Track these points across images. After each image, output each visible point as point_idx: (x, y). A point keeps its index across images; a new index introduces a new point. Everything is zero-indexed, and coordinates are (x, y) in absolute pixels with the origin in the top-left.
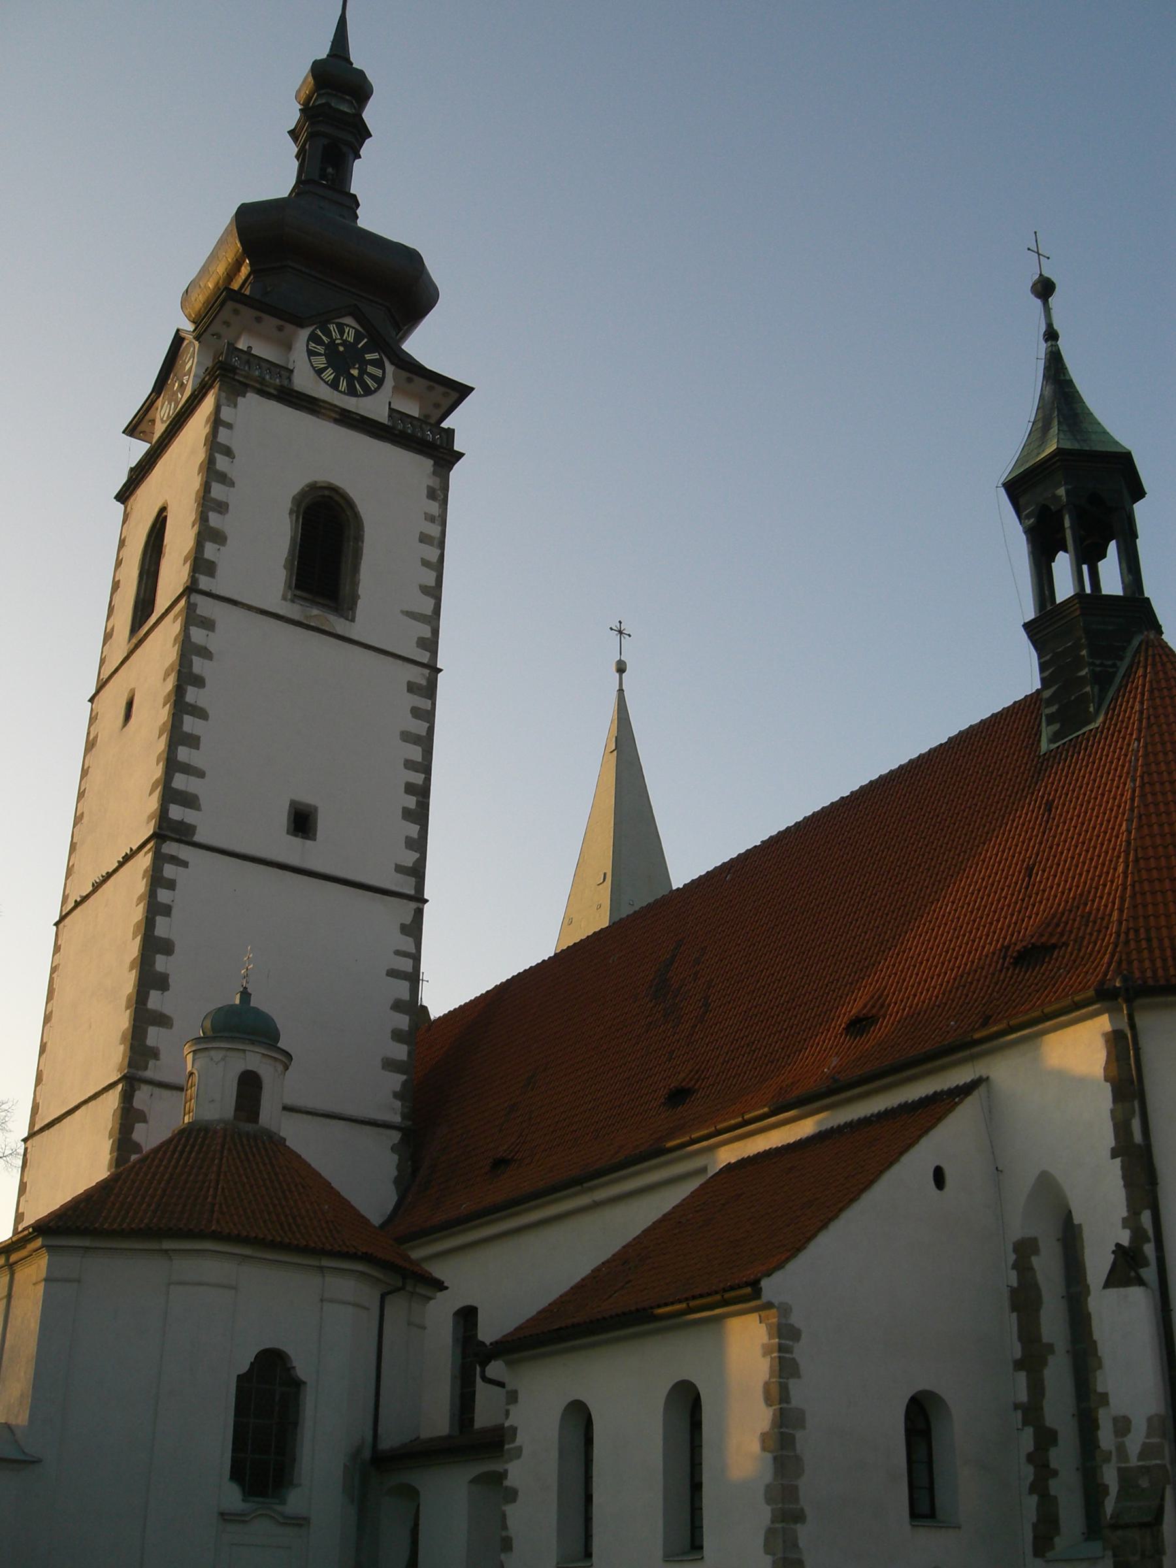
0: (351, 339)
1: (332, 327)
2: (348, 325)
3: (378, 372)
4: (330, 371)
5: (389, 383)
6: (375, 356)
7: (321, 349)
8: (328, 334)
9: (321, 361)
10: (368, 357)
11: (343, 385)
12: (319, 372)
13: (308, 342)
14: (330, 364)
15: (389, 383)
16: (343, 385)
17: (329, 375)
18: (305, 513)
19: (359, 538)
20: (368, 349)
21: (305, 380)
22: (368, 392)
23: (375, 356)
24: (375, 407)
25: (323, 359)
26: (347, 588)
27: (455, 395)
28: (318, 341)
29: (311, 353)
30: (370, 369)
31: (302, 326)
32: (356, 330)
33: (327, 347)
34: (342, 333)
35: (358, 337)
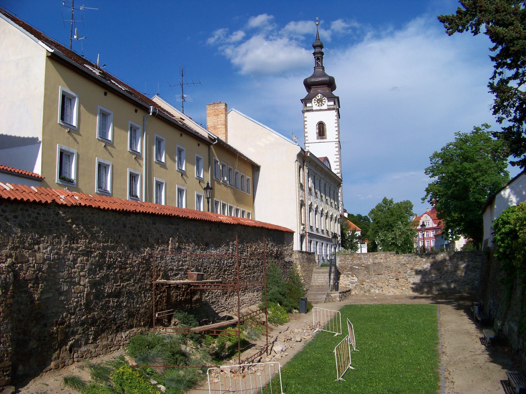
6: (324, 98)
8: (316, 98)
11: (320, 105)
12: (316, 105)
15: (327, 101)
16: (320, 105)
20: (322, 98)
22: (323, 104)
29: (315, 103)
30: (324, 101)
35: (321, 96)
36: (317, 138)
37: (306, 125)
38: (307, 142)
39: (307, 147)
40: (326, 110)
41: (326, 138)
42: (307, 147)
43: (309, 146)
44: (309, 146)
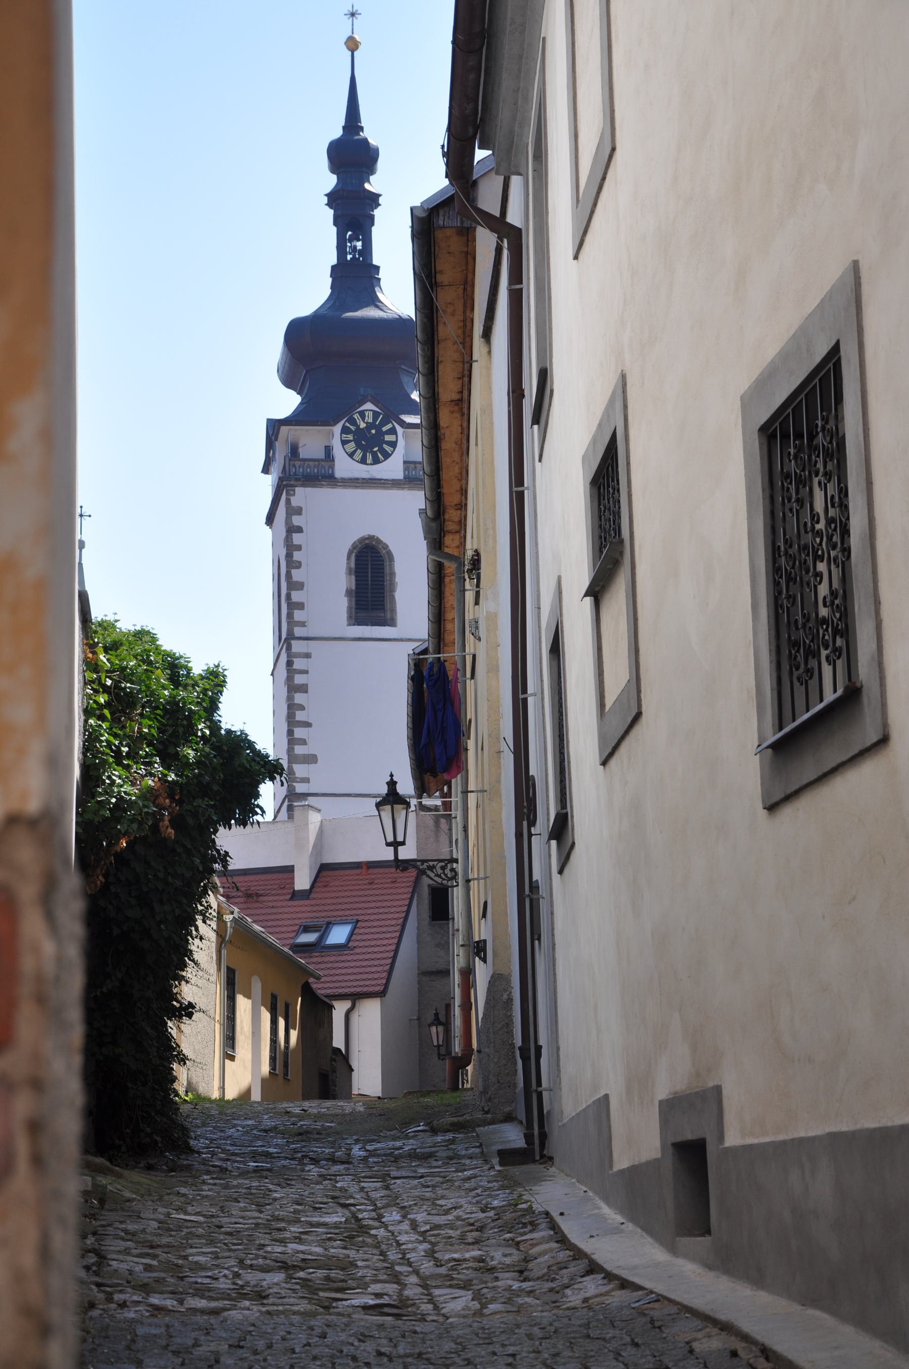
0: (371, 420)
1: (356, 416)
2: (367, 410)
4: (359, 451)
5: (401, 443)
6: (389, 426)
7: (350, 437)
8: (353, 421)
9: (351, 446)
10: (384, 429)
11: (369, 459)
12: (351, 455)
14: (359, 446)
16: (369, 459)
17: (359, 455)
22: (387, 456)
23: (389, 426)
25: (353, 444)
29: (344, 443)
30: (388, 438)
31: (335, 423)
32: (374, 412)
34: (363, 418)
35: (376, 415)
36: (350, 617)
37: (299, 548)
38: (298, 631)
39: (299, 655)
40: (394, 484)
41: (391, 622)
42: (299, 655)
43: (308, 656)
44: (308, 656)
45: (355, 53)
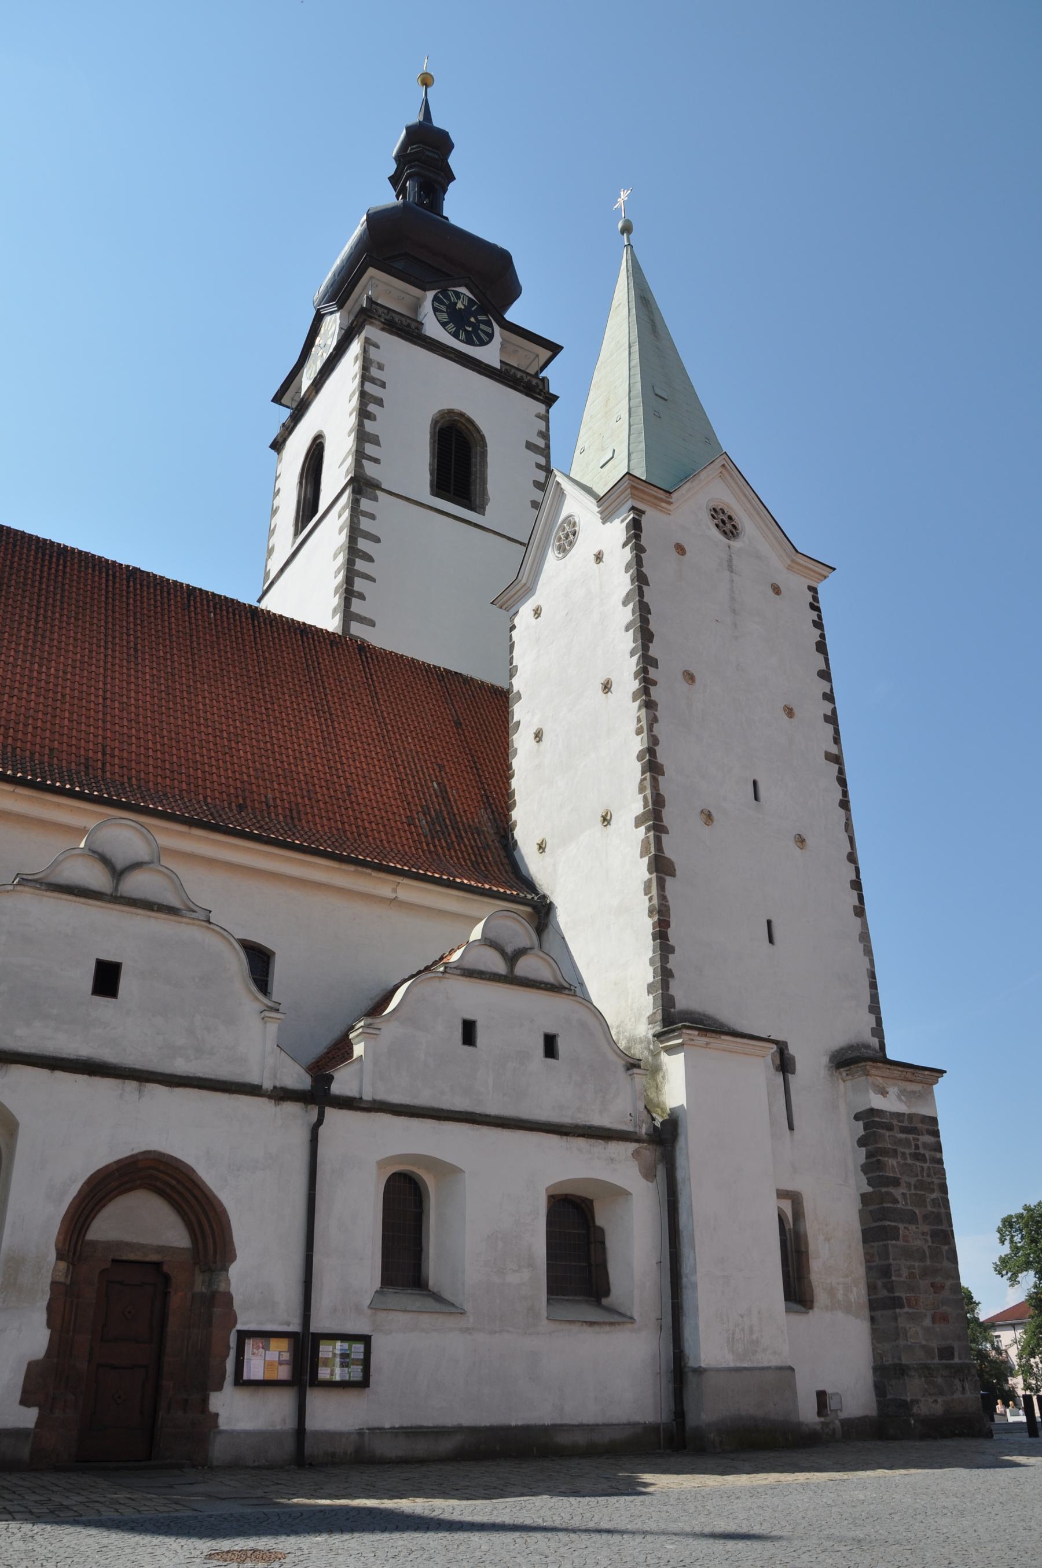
3: (489, 330)
8: (448, 298)
9: (445, 317)
12: (444, 325)
13: (433, 301)
18: (439, 432)
19: (484, 454)
21: (433, 328)
22: (483, 343)
24: (490, 354)
26: (478, 486)
27: (546, 354)
28: (441, 302)
29: (436, 310)
30: (482, 326)
32: (469, 298)
33: (448, 307)
45: (428, 89)
